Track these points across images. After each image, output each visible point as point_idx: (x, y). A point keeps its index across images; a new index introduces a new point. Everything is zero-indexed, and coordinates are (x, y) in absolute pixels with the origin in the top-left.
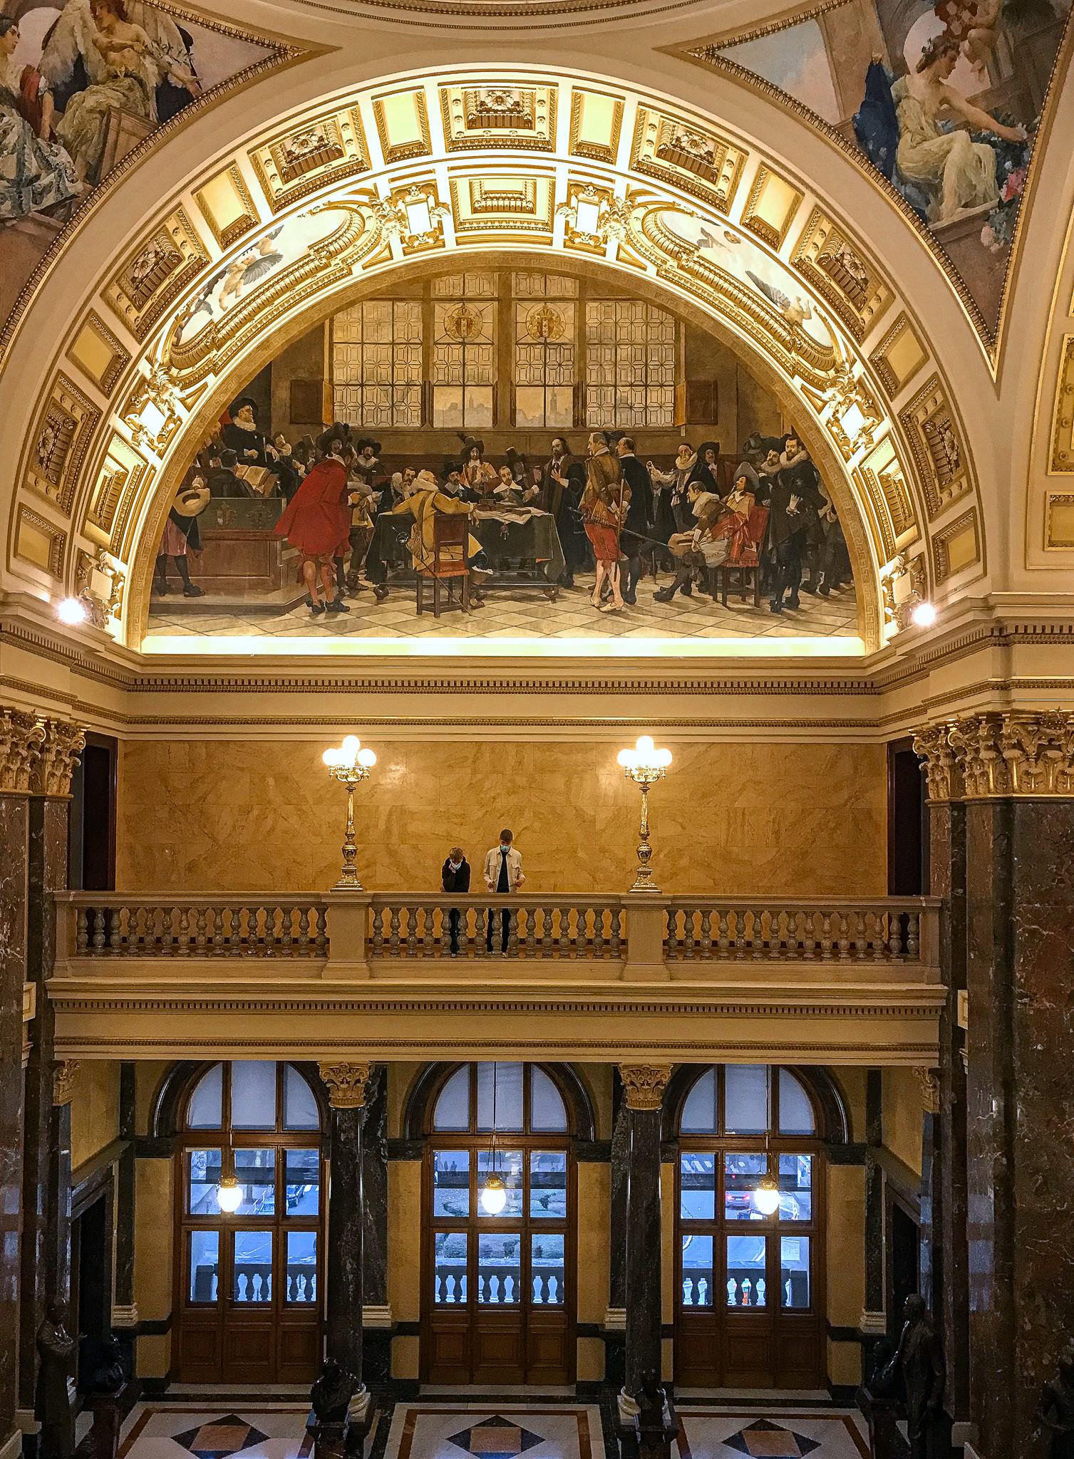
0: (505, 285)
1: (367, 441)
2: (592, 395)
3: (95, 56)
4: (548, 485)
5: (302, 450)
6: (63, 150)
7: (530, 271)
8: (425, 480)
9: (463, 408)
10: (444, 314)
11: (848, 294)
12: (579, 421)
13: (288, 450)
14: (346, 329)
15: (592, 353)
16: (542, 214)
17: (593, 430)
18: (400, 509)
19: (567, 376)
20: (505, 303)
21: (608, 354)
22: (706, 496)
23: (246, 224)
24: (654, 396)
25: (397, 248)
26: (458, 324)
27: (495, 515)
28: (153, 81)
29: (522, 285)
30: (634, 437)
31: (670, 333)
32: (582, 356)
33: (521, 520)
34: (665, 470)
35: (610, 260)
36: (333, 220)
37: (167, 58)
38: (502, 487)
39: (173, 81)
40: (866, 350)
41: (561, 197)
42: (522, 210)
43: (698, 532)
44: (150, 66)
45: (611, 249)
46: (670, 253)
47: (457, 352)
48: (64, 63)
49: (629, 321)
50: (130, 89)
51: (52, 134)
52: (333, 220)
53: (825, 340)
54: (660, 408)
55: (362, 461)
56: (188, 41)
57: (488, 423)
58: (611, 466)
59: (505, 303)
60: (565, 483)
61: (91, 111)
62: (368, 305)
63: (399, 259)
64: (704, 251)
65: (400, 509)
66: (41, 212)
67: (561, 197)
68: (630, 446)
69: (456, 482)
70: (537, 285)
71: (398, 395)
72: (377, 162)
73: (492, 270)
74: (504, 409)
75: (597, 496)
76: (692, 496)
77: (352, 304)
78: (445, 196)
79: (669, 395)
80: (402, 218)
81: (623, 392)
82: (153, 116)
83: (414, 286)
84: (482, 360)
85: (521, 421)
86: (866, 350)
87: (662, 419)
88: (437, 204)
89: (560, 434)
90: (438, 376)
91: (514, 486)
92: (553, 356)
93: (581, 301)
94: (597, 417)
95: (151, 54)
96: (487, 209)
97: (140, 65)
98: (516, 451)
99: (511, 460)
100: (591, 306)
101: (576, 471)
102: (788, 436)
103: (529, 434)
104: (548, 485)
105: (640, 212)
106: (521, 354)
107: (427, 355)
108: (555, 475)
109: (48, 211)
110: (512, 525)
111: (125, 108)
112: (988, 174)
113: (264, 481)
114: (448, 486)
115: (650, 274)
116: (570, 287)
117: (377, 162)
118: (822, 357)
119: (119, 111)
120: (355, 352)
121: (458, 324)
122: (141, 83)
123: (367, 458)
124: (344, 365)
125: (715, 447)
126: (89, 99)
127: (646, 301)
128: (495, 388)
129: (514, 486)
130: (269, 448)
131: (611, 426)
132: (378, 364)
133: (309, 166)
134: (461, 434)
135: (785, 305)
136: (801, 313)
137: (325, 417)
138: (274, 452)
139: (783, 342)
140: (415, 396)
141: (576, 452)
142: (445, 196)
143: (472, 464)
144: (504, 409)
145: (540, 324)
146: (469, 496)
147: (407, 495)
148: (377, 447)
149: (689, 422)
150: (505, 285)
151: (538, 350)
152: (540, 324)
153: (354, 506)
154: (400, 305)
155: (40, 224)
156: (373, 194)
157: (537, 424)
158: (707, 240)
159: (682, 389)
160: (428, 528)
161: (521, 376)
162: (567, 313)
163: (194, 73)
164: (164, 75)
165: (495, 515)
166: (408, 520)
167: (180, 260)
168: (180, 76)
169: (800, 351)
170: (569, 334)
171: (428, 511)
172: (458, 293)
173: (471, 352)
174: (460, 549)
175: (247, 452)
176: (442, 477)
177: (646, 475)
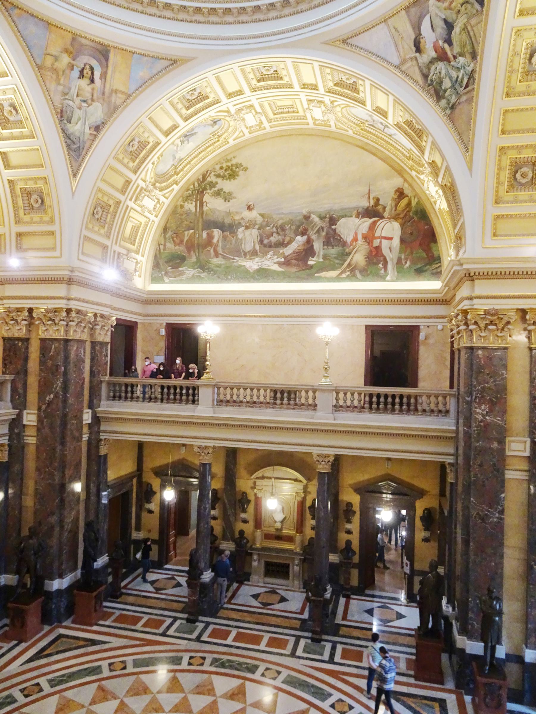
3: (449, 12)
48: (443, 28)
50: (466, 9)
61: (460, 33)
66: (465, 88)
109: (467, 86)
111: (469, 18)
119: (468, 21)
126: (457, 29)
155: (467, 93)
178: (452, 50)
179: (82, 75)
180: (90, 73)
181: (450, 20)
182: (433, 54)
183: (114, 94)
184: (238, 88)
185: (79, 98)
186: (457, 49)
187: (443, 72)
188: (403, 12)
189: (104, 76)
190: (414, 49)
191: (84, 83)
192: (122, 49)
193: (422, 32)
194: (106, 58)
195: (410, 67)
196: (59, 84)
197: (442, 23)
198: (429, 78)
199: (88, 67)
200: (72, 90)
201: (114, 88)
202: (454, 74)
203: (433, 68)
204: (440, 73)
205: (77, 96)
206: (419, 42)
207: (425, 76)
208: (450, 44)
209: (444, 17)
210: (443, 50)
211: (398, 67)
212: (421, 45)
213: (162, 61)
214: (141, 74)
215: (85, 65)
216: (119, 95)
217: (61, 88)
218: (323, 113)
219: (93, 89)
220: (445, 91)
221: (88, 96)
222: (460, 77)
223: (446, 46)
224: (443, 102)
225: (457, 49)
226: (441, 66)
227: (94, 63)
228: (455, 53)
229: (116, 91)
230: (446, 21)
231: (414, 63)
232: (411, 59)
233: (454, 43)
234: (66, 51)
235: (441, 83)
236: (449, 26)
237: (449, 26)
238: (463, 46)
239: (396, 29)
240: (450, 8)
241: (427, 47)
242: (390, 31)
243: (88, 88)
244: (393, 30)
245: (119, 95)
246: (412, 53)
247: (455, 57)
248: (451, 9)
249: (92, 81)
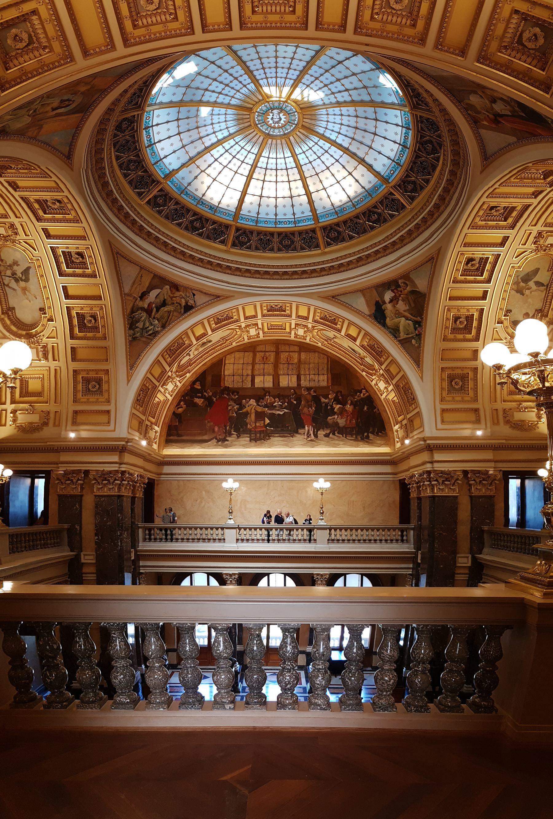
0: (277, 348)
1: (234, 391)
2: (302, 377)
4: (290, 403)
5: (214, 394)
7: (285, 344)
8: (252, 402)
9: (264, 381)
10: (259, 356)
11: (377, 354)
12: (299, 384)
13: (211, 394)
14: (229, 360)
15: (302, 366)
16: (288, 330)
17: (303, 387)
18: (244, 410)
19: (295, 372)
20: (277, 353)
21: (307, 366)
22: (339, 406)
23: (204, 335)
24: (321, 377)
25: (246, 338)
26: (263, 358)
27: (274, 412)
28: (183, 304)
29: (282, 348)
30: (316, 389)
31: (326, 361)
32: (299, 367)
33: (281, 413)
34: (326, 399)
35: (308, 341)
36: (228, 332)
38: (276, 404)
39: (189, 304)
40: (383, 367)
41: (293, 326)
42: (282, 329)
43: (336, 416)
44: (183, 300)
45: (308, 338)
46: (325, 340)
47: (262, 366)
49: (314, 358)
52: (228, 332)
53: (372, 363)
54: (323, 380)
55: (233, 397)
56: (194, 295)
57: (271, 385)
58: (309, 397)
59: (277, 353)
60: (295, 402)
62: (237, 353)
63: (246, 340)
64: (335, 340)
65: (244, 410)
67: (293, 326)
68: (315, 392)
69: (262, 402)
70: (287, 348)
71: (244, 378)
72: (242, 319)
73: (274, 344)
74: (276, 381)
75: (305, 406)
76: (334, 406)
77: (232, 353)
78: (260, 326)
79: (326, 377)
80: (248, 332)
81: (312, 376)
82: (182, 312)
83: (251, 348)
84: (269, 368)
85: (281, 385)
86: (383, 367)
87: (324, 384)
88: (258, 328)
89: (293, 388)
90: (256, 372)
91: (280, 403)
92: (290, 367)
93: (299, 353)
94: (303, 383)
96: (272, 329)
97: (181, 301)
98: (279, 393)
99: (279, 396)
100: (302, 353)
101: (299, 399)
102: (362, 389)
103: (284, 388)
104: (290, 403)
105: (316, 331)
106: (281, 366)
107: (253, 367)
108: (292, 400)
110: (279, 414)
112: (412, 326)
113: (203, 402)
114: (260, 403)
115: (320, 345)
116: (296, 348)
117: (242, 319)
118: (371, 367)
120: (232, 366)
121: (263, 358)
122: (180, 305)
123: (235, 396)
124: (228, 370)
125: (341, 392)
126: (166, 309)
127: (319, 352)
128: (273, 376)
129: (280, 403)
130: (205, 393)
131: (309, 386)
132: (238, 370)
133: (222, 321)
134: (264, 389)
135: (360, 354)
136: (364, 356)
137: (222, 385)
138: (206, 394)
139: (359, 363)
140: (249, 378)
141: (299, 393)
142: (260, 326)
143: (267, 397)
144: (276, 381)
145: (287, 358)
146: (266, 406)
147: (247, 406)
148: (238, 393)
149: (332, 385)
150: (277, 348)
151: (286, 365)
152: (287, 358)
153: (230, 410)
154: (246, 354)
156: (240, 326)
157: (286, 386)
158: (335, 337)
159: (330, 375)
160: (253, 416)
161: (281, 372)
162: (296, 355)
165: (274, 412)
166: (247, 414)
167: (185, 344)
168: (191, 302)
169: (364, 366)
170: (296, 361)
171: (253, 411)
172: (264, 350)
173: (266, 366)
174: (263, 422)
175: (198, 395)
176: (257, 401)
177: (320, 400)
178: (155, 314)
181: (167, 302)
182: (146, 306)
190: (140, 295)
195: (130, 300)
197: (162, 299)
206: (145, 295)
208: (157, 311)
210: (152, 310)
212: (145, 297)
223: (155, 309)
225: (158, 316)
226: (144, 315)
228: (156, 316)
231: (134, 300)
232: (134, 297)
233: (159, 312)
236: (164, 304)
238: (162, 317)
240: (172, 298)
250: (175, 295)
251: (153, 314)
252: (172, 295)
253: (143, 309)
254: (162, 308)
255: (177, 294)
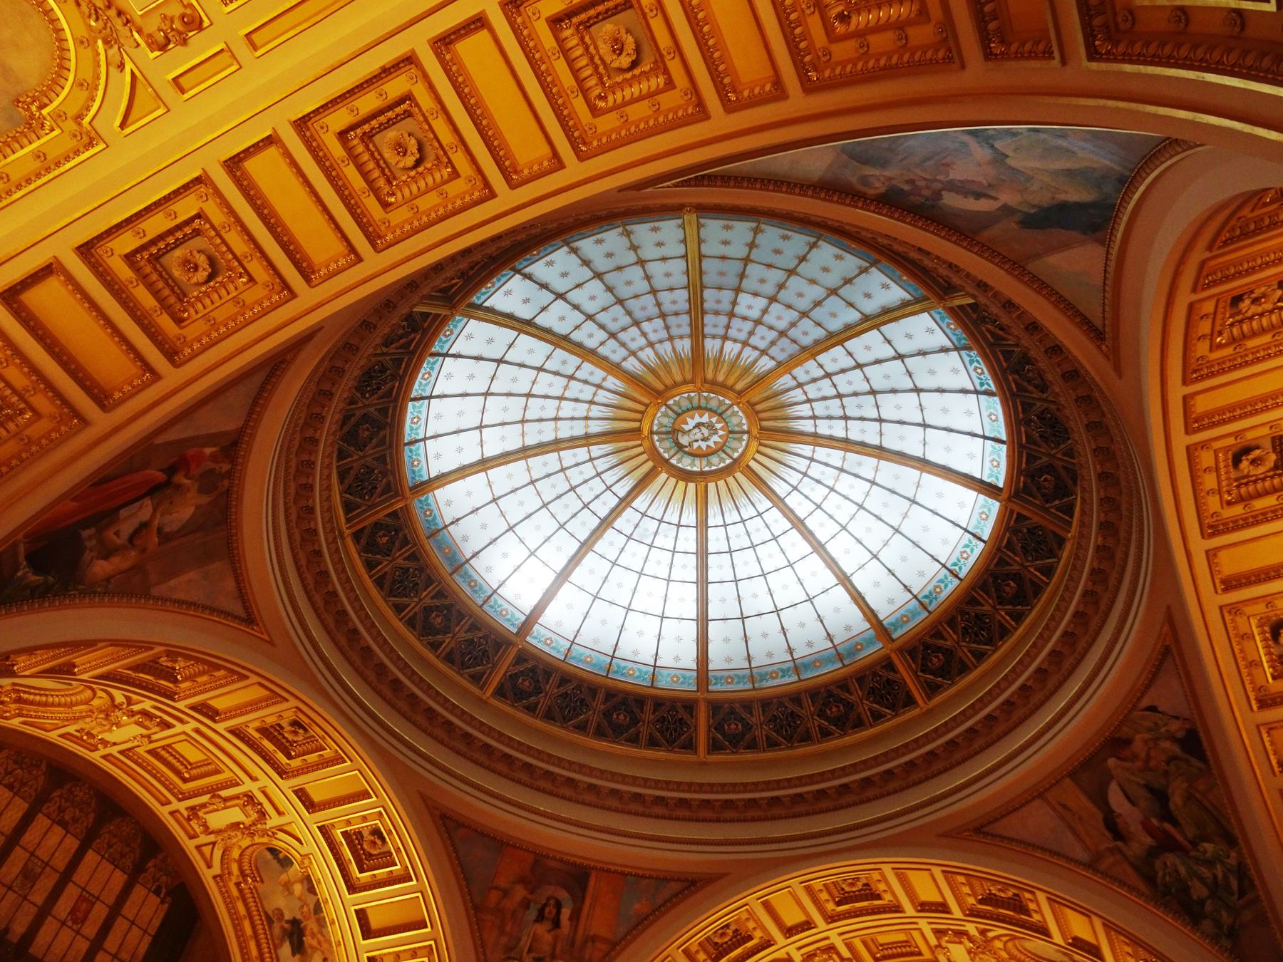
6: (1206, 845)
28: (1177, 750)
37: (1163, 730)
39: (1180, 735)
44: (1166, 744)
51: (1191, 842)
56: (1153, 709)
95: (1158, 739)
109: (1242, 893)
122: (1175, 758)
126: (1176, 800)
163: (1177, 718)
164: (1173, 738)
179: (540, 918)
180: (554, 911)
182: (1149, 840)
183: (590, 944)
184: (803, 918)
185: (533, 955)
186: (1191, 832)
187: (1182, 870)
188: (1068, 781)
189: (575, 916)
191: (542, 929)
192: (609, 871)
193: (1114, 808)
194: (584, 887)
196: (502, 933)
198: (1159, 881)
199: (552, 902)
200: (522, 943)
201: (591, 933)
202: (1204, 871)
203: (1158, 864)
204: (1177, 871)
205: (530, 951)
207: (1150, 879)
209: (1143, 782)
210: (1165, 832)
211: (1091, 866)
213: (673, 884)
214: (637, 906)
215: (548, 899)
216: (598, 945)
217: (504, 940)
218: (969, 952)
219: (556, 938)
220: (1202, 903)
221: (547, 948)
222: (1220, 875)
223: (1167, 826)
224: (1207, 925)
226: (1171, 859)
227: (563, 895)
228: (1190, 835)
229: (594, 939)
230: (1149, 788)
232: (1111, 851)
234: (522, 880)
235: (1186, 890)
236: (1160, 796)
237: (1160, 796)
239: (1064, 806)
241: (1132, 829)
242: (1054, 810)
243: (548, 938)
244: (1060, 809)
245: (598, 945)
246: (1107, 843)
247: (1194, 844)
248: (1150, 770)
249: (556, 924)
250: (1143, 755)
251: (1178, 837)
252: (1139, 764)
253: (1152, 853)
254: (1172, 806)
255: (1138, 746)
